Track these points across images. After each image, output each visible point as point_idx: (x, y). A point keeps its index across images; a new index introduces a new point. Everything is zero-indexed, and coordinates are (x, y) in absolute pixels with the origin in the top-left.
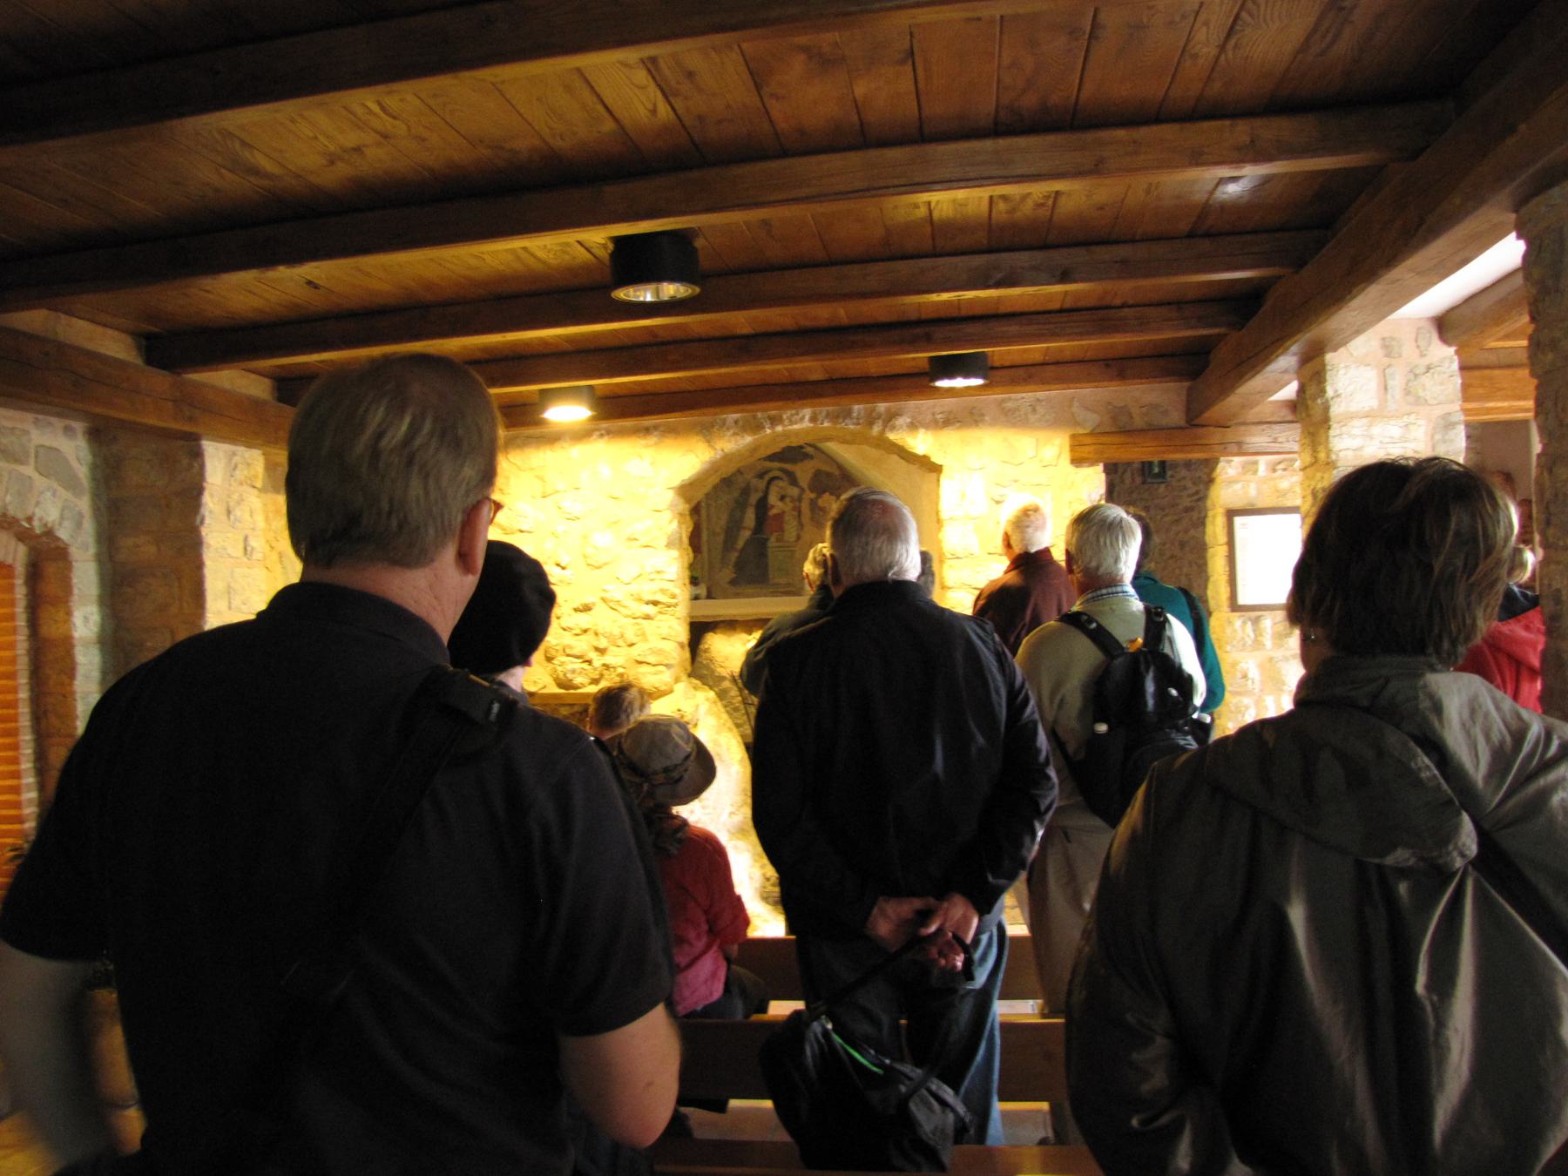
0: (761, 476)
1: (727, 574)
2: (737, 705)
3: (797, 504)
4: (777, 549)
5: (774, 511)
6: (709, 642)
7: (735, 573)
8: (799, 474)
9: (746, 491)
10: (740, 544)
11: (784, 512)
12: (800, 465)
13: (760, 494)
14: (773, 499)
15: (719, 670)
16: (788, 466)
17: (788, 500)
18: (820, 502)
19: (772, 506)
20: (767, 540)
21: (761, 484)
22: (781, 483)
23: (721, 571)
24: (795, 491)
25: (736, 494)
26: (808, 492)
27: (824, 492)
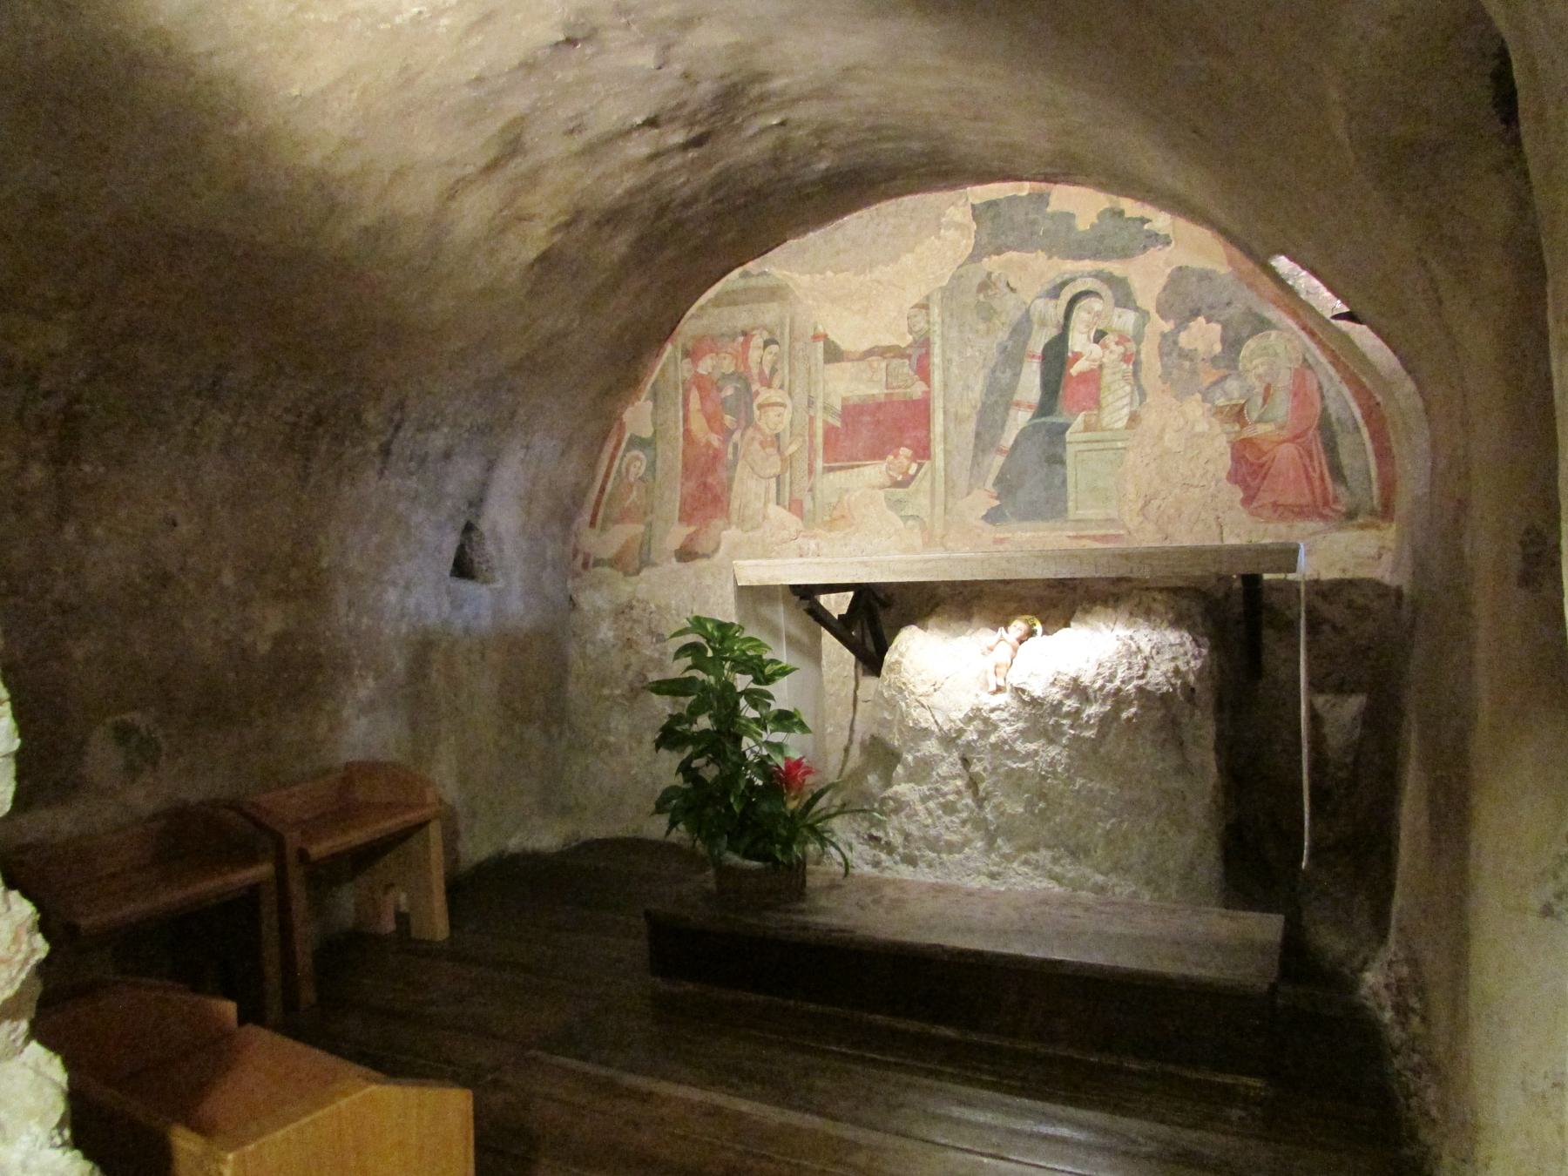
0: (1055, 292)
1: (983, 499)
2: (951, 797)
3: (1132, 347)
4: (1090, 446)
5: (1075, 370)
6: (902, 648)
7: (997, 498)
8: (1136, 283)
9: (1021, 329)
10: (1008, 439)
11: (1101, 367)
12: (1141, 259)
13: (1052, 332)
14: (1078, 341)
15: (916, 713)
16: (1114, 267)
17: (1110, 339)
18: (1184, 339)
19: (1077, 356)
20: (1065, 427)
21: (1056, 309)
22: (1097, 305)
23: (968, 494)
24: (1126, 320)
25: (1003, 335)
26: (1155, 316)
27: (1195, 314)
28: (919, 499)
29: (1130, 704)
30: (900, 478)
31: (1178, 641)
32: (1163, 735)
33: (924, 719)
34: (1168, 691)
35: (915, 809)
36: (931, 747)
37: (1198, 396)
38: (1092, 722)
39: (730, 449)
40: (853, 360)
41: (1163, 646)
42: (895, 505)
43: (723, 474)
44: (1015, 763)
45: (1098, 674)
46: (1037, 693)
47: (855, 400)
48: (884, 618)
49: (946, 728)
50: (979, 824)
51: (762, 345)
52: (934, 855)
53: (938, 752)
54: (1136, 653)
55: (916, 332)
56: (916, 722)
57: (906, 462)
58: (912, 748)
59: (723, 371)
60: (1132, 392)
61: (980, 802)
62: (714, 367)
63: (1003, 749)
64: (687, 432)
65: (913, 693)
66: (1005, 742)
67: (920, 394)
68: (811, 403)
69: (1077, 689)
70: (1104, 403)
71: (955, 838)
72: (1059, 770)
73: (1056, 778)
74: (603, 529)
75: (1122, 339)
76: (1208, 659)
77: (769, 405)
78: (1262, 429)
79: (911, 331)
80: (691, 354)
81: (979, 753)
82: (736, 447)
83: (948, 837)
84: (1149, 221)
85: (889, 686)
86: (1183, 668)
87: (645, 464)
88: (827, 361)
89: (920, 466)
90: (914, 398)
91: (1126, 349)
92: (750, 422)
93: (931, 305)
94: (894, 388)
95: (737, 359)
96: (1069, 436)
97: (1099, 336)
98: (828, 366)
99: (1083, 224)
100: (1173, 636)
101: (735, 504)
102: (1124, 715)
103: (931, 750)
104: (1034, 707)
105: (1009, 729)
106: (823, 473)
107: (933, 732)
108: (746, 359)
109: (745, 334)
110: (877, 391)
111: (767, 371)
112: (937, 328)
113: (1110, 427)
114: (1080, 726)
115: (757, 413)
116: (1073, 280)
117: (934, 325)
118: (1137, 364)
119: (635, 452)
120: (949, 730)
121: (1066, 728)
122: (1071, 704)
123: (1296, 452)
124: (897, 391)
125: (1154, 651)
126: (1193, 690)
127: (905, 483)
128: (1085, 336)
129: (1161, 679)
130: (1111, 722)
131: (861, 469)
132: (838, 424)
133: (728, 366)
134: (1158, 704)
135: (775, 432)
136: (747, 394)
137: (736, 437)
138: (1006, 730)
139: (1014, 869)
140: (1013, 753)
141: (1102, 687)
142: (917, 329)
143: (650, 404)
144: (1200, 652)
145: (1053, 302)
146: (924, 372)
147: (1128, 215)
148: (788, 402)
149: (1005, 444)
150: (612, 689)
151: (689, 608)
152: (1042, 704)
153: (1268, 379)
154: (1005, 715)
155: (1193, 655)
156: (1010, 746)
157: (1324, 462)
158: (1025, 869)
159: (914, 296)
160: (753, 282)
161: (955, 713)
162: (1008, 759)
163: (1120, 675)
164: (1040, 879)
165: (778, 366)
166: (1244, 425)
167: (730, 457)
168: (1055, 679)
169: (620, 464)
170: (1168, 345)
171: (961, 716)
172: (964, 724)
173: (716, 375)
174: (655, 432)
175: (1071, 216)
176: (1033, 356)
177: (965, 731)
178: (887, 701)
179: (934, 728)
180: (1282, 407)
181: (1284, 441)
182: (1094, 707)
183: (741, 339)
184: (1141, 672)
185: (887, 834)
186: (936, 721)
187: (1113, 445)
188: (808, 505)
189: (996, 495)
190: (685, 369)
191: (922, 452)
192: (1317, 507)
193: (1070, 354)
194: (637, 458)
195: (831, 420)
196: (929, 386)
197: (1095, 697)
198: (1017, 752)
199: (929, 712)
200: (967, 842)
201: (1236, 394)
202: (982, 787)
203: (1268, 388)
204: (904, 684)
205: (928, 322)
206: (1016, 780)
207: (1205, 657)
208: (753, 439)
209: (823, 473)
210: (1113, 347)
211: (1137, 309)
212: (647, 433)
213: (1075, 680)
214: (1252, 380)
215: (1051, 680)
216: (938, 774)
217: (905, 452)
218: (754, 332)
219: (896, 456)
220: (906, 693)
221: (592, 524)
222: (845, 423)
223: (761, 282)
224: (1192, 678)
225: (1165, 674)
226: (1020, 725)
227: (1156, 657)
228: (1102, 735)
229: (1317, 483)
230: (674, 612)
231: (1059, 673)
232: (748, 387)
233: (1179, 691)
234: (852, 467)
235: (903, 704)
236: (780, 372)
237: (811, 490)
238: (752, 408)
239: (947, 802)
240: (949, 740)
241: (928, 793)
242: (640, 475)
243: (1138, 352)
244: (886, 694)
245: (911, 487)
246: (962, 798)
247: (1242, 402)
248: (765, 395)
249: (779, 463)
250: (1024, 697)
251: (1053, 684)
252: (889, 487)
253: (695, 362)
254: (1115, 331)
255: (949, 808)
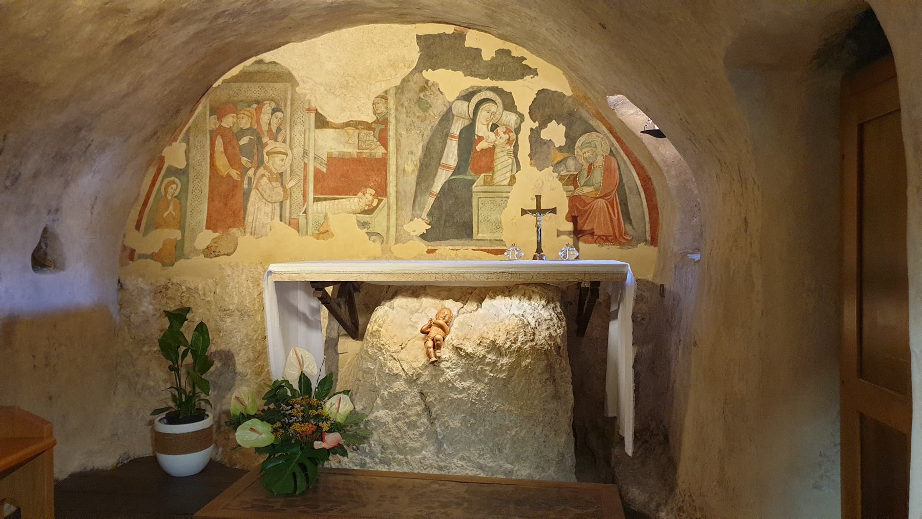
0: (467, 97)
1: (421, 226)
2: (413, 418)
3: (513, 136)
5: (479, 147)
7: (429, 225)
9: (447, 117)
10: (437, 188)
11: (494, 147)
13: (467, 122)
14: (481, 129)
17: (501, 130)
19: (481, 139)
22: (493, 107)
24: (510, 118)
26: (527, 116)
28: (379, 221)
29: (527, 357)
30: (366, 208)
31: (549, 317)
32: (548, 376)
33: (395, 367)
34: (548, 348)
35: (389, 427)
36: (400, 385)
37: (551, 168)
38: (504, 368)
39: (246, 181)
40: (336, 128)
41: (542, 321)
42: (363, 225)
43: (239, 196)
44: (456, 395)
45: (507, 339)
46: (470, 350)
47: (335, 155)
48: (358, 298)
49: (410, 373)
50: (432, 435)
51: (270, 111)
52: (403, 457)
53: (405, 389)
54: (527, 325)
55: (379, 114)
56: (390, 370)
57: (371, 198)
58: (387, 387)
59: (241, 127)
60: (513, 163)
61: (432, 421)
62: (234, 123)
63: (448, 386)
64: (213, 165)
65: (389, 351)
66: (449, 381)
67: (381, 154)
68: (306, 153)
69: (494, 347)
70: (495, 170)
71: (417, 445)
72: (484, 398)
73: (481, 404)
74: (146, 233)
75: (508, 131)
76: (566, 328)
77: (275, 153)
78: (587, 190)
79: (375, 113)
80: (218, 111)
81: (432, 389)
82: (250, 179)
83: (412, 444)
84: (526, 59)
85: (373, 346)
86: (554, 334)
87: (180, 187)
88: (317, 127)
89: (380, 201)
90: (376, 157)
91: (510, 137)
92: (261, 163)
93: (389, 97)
94: (363, 149)
95: (252, 118)
96: (475, 188)
97: (494, 127)
98: (318, 131)
99: (487, 55)
100: (545, 314)
101: (249, 219)
102: (523, 364)
103: (400, 388)
104: (467, 360)
105: (451, 373)
106: (314, 202)
107: (401, 376)
108: (258, 121)
109: (257, 102)
110: (351, 150)
111: (274, 130)
112: (392, 112)
113: (499, 184)
114: (496, 371)
115: (266, 157)
116: (480, 91)
117: (390, 109)
118: (516, 146)
119: (173, 178)
120: (412, 375)
121: (488, 372)
122: (491, 357)
123: (605, 204)
124: (364, 151)
125: (537, 324)
126: (560, 347)
127: (370, 211)
128: (486, 126)
129: (543, 341)
130: (516, 369)
131: (340, 200)
132: (324, 170)
133: (245, 123)
134: (543, 357)
135: (279, 172)
136: (258, 143)
137: (251, 173)
138: (449, 374)
139: (455, 464)
140: (454, 388)
141: (511, 346)
142: (378, 112)
143: (184, 145)
144: (561, 326)
145: (467, 103)
146: (384, 142)
147: (512, 55)
148: (289, 152)
149: (435, 191)
150: (150, 347)
151: (213, 290)
152: (471, 357)
153: (591, 161)
154: (449, 364)
155: (558, 326)
156: (453, 384)
157: (620, 210)
158: (463, 463)
159: (379, 89)
160: (264, 67)
161: (415, 363)
162: (451, 393)
163: (521, 338)
164: (471, 469)
165: (281, 127)
166: (576, 187)
167: (246, 186)
168: (481, 342)
169: (159, 189)
170: (535, 134)
171: (420, 365)
172: (422, 370)
173: (235, 130)
174: (188, 165)
175: (478, 51)
176: (455, 137)
177: (423, 375)
178: (370, 357)
179: (402, 373)
180: (598, 177)
181: (597, 198)
182: (505, 359)
183: (255, 106)
184: (532, 337)
185: (370, 445)
186: (403, 369)
187: (500, 195)
188: (302, 222)
189: (428, 222)
190: (212, 123)
191: (381, 191)
192: (616, 238)
193: (476, 137)
194: (174, 182)
195: (318, 166)
196: (387, 150)
197: (506, 353)
198: (457, 388)
199: (398, 363)
200: (424, 446)
201: (573, 169)
202: (433, 410)
203: (591, 165)
204: (383, 345)
205: (387, 108)
206: (457, 405)
207: (564, 327)
208: (263, 175)
209: (314, 202)
210: (502, 134)
211: (516, 112)
212: (182, 165)
213: (494, 342)
214: (582, 161)
215: (478, 342)
216: (405, 404)
217: (371, 191)
218: (265, 102)
219: (364, 194)
220: (384, 351)
221: (138, 227)
222: (328, 169)
223: (271, 68)
224: (559, 340)
225: (544, 338)
226: (459, 370)
227: (538, 328)
228: (510, 377)
229: (616, 223)
230: (201, 293)
231: (483, 338)
232: (259, 139)
233: (553, 348)
234: (334, 199)
235: (381, 358)
236: (283, 131)
237: (305, 212)
238: (262, 154)
239: (410, 421)
240: (412, 381)
241: (398, 416)
242: (175, 195)
243: (517, 138)
244: (370, 352)
245: (373, 215)
246: (421, 418)
247: (576, 173)
248: (271, 146)
249: (282, 193)
250: (461, 353)
251: (479, 345)
252: (359, 213)
253: (220, 118)
254: (504, 125)
255: (412, 425)
